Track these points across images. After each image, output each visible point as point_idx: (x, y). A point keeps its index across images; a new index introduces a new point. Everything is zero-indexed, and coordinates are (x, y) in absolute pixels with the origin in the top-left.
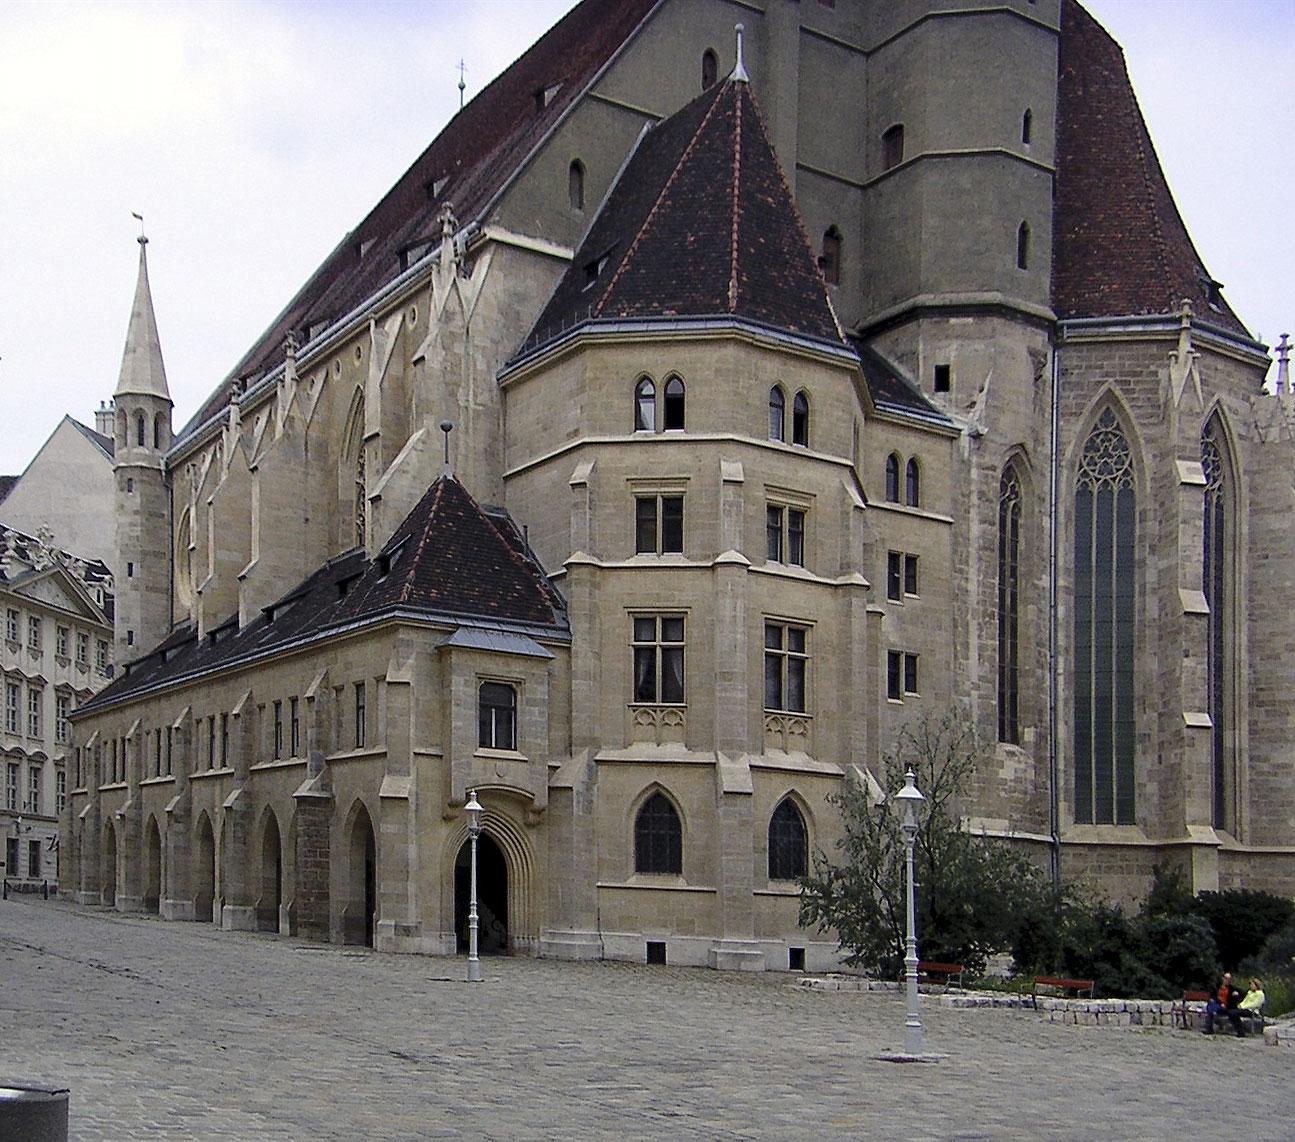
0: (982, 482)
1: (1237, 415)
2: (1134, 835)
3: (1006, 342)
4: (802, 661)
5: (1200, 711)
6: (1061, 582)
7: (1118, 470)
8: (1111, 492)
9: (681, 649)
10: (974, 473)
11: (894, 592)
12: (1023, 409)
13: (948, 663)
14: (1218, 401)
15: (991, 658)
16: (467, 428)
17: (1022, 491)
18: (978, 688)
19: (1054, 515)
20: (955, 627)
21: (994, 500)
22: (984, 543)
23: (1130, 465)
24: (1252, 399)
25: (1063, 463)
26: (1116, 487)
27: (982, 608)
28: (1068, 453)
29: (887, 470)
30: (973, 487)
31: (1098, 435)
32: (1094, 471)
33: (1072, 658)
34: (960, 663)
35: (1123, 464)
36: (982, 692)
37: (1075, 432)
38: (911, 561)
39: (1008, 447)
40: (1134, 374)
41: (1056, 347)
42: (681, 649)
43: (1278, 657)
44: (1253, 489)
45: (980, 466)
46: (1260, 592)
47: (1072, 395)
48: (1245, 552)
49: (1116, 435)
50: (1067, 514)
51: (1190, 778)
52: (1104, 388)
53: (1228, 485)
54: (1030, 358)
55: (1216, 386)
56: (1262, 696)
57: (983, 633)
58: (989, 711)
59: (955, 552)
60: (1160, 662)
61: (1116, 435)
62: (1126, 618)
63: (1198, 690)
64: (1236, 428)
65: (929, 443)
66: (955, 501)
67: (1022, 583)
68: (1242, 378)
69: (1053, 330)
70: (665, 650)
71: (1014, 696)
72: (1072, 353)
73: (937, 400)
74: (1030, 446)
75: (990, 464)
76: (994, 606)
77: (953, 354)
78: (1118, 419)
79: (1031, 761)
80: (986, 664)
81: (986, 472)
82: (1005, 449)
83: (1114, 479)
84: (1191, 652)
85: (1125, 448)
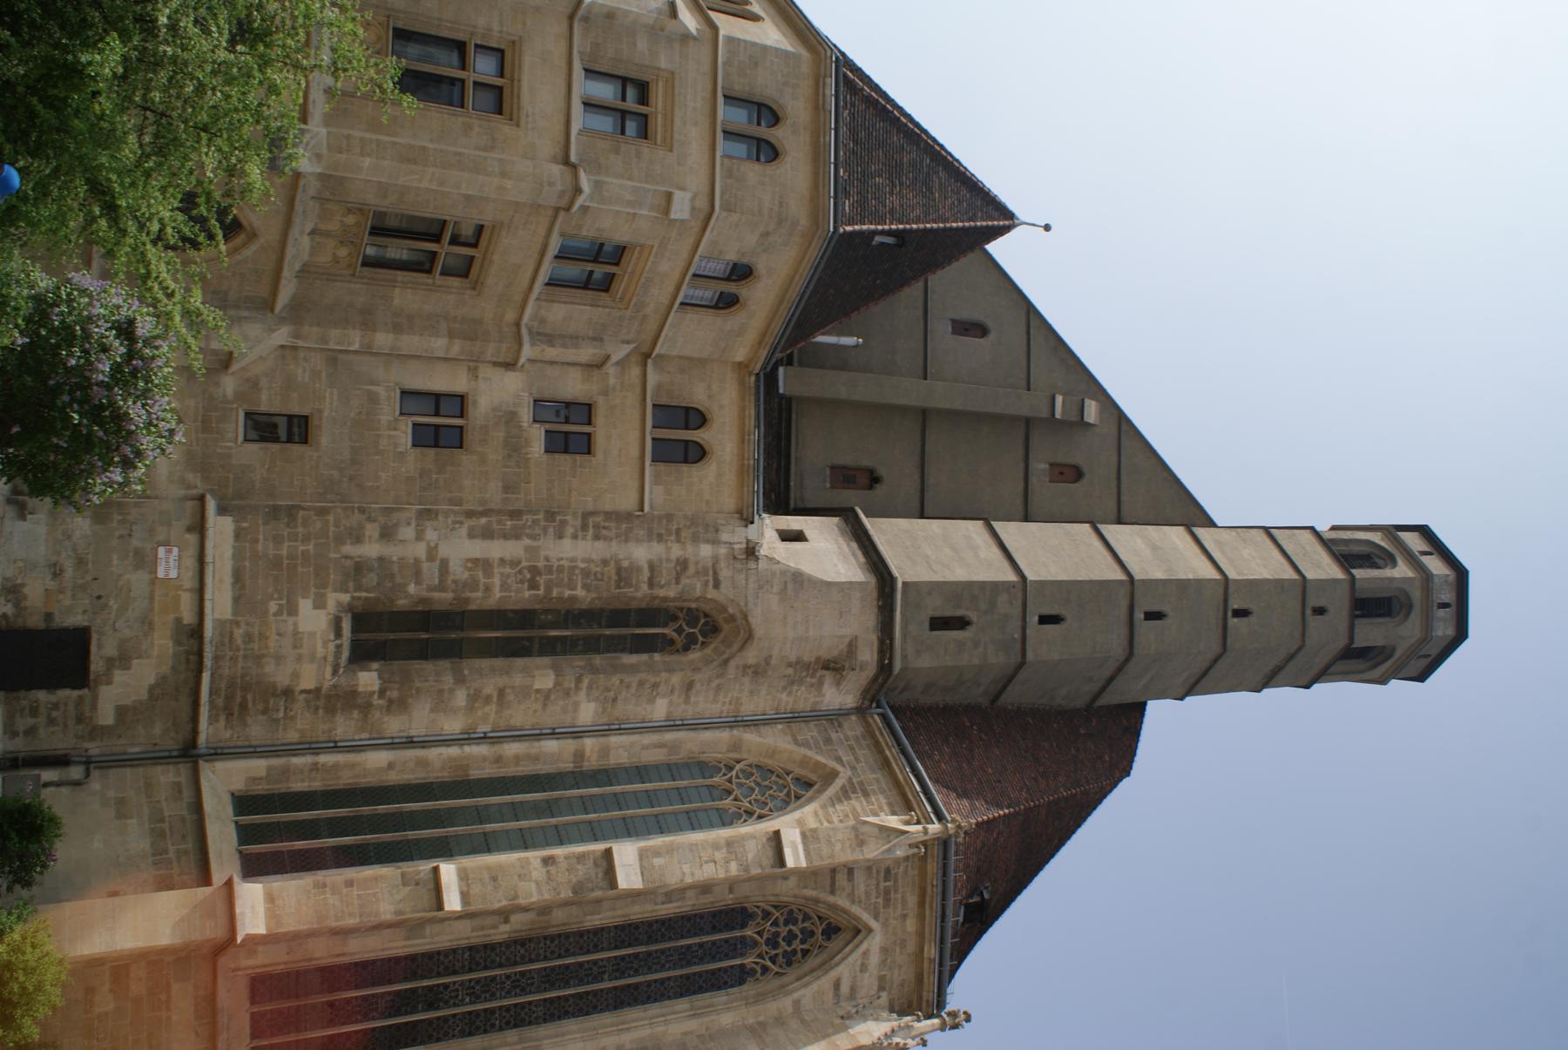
0: (697, 563)
1: (861, 971)
5: (465, 896)
6: (589, 743)
7: (750, 802)
10: (706, 551)
11: (544, 408)
13: (459, 502)
14: (870, 931)
15: (472, 584)
17: (694, 655)
18: (432, 554)
19: (672, 725)
20: (516, 514)
21: (680, 587)
22: (626, 569)
24: (884, 995)
25: (735, 732)
27: (541, 564)
28: (750, 737)
30: (690, 549)
32: (738, 777)
34: (461, 523)
36: (425, 566)
38: (585, 445)
39: (744, 609)
41: (860, 711)
44: (780, 1021)
45: (716, 560)
47: (815, 734)
49: (788, 794)
50: (673, 747)
52: (839, 768)
53: (777, 982)
54: (843, 646)
55: (885, 925)
57: (508, 570)
58: (398, 580)
59: (608, 515)
63: (496, 888)
64: (844, 971)
65: (730, 477)
66: (669, 517)
67: (579, 661)
68: (903, 973)
71: (425, 652)
72: (859, 730)
74: (751, 656)
75: (721, 579)
76: (549, 588)
79: (329, 680)
80: (466, 575)
81: (711, 573)
82: (742, 604)
83: (736, 799)
84: (553, 869)
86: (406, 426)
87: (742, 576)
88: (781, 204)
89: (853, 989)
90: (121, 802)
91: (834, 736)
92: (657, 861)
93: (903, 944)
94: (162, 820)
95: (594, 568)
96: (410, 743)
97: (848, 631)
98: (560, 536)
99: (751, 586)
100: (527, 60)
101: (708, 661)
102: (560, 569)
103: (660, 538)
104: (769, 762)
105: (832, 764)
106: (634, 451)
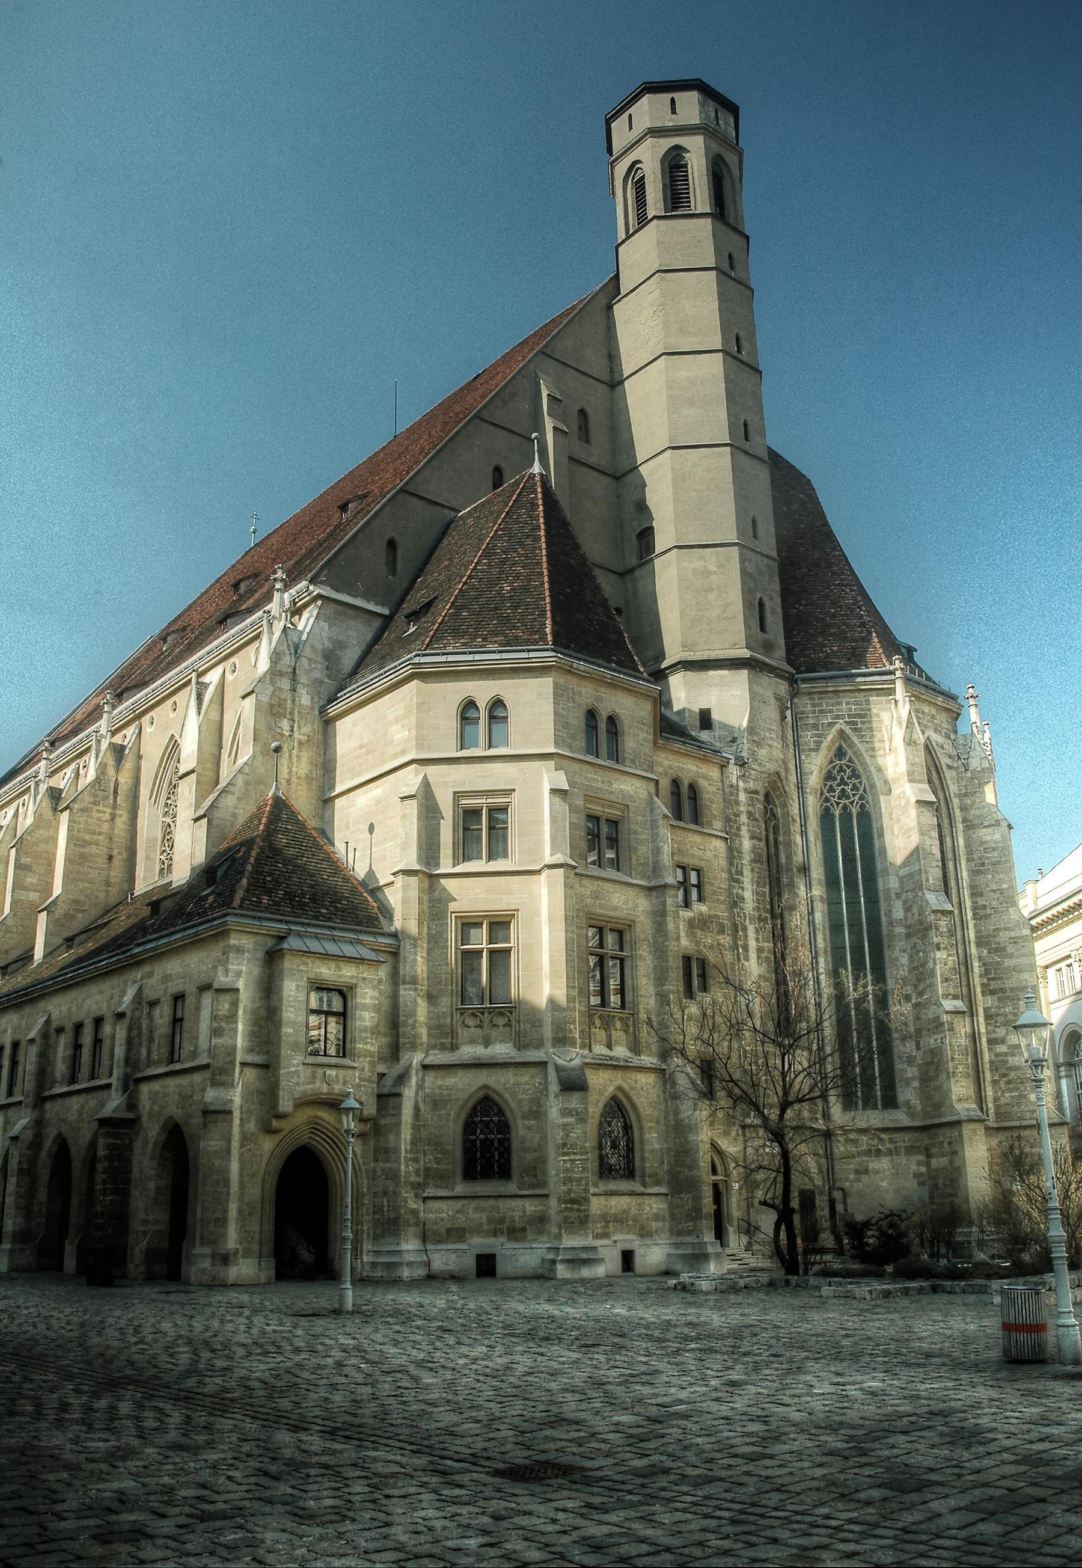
2: (900, 1117)
3: (757, 689)
4: (622, 961)
5: (955, 997)
7: (854, 795)
8: (850, 815)
9: (508, 951)
10: (742, 797)
12: (775, 744)
15: (767, 959)
16: (290, 756)
17: (779, 811)
20: (735, 928)
23: (864, 791)
26: (854, 811)
29: (672, 793)
30: (742, 808)
31: (834, 768)
33: (830, 959)
35: (858, 790)
37: (816, 765)
40: (860, 716)
42: (508, 951)
43: (1004, 949)
44: (963, 809)
45: (746, 790)
46: (981, 895)
48: (963, 862)
49: (849, 767)
51: (953, 1059)
56: (993, 985)
59: (731, 864)
60: (911, 957)
61: (849, 767)
62: (874, 921)
69: (792, 681)
70: (492, 952)
72: (805, 700)
73: (704, 735)
74: (783, 774)
77: (714, 698)
78: (850, 753)
83: (852, 803)
84: (942, 946)
85: (858, 777)
86: (699, 995)
87: (753, 772)
88: (643, 723)
89: (950, 757)
90: (857, 1172)
91: (811, 721)
92: (931, 882)
93: (933, 717)
94: (870, 1150)
95: (755, 879)
96: (818, 1005)
97: (772, 700)
98: (743, 898)
99: (756, 767)
100: (598, 911)
101: (784, 805)
102: (758, 902)
103: (739, 829)
104: (824, 772)
105: (833, 732)
106: (697, 838)
